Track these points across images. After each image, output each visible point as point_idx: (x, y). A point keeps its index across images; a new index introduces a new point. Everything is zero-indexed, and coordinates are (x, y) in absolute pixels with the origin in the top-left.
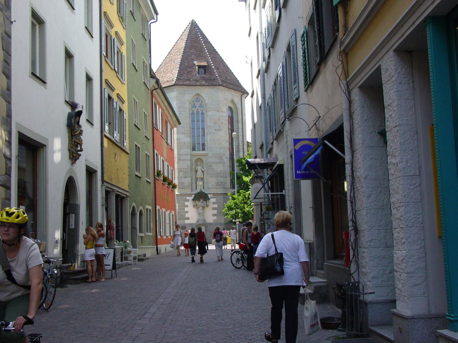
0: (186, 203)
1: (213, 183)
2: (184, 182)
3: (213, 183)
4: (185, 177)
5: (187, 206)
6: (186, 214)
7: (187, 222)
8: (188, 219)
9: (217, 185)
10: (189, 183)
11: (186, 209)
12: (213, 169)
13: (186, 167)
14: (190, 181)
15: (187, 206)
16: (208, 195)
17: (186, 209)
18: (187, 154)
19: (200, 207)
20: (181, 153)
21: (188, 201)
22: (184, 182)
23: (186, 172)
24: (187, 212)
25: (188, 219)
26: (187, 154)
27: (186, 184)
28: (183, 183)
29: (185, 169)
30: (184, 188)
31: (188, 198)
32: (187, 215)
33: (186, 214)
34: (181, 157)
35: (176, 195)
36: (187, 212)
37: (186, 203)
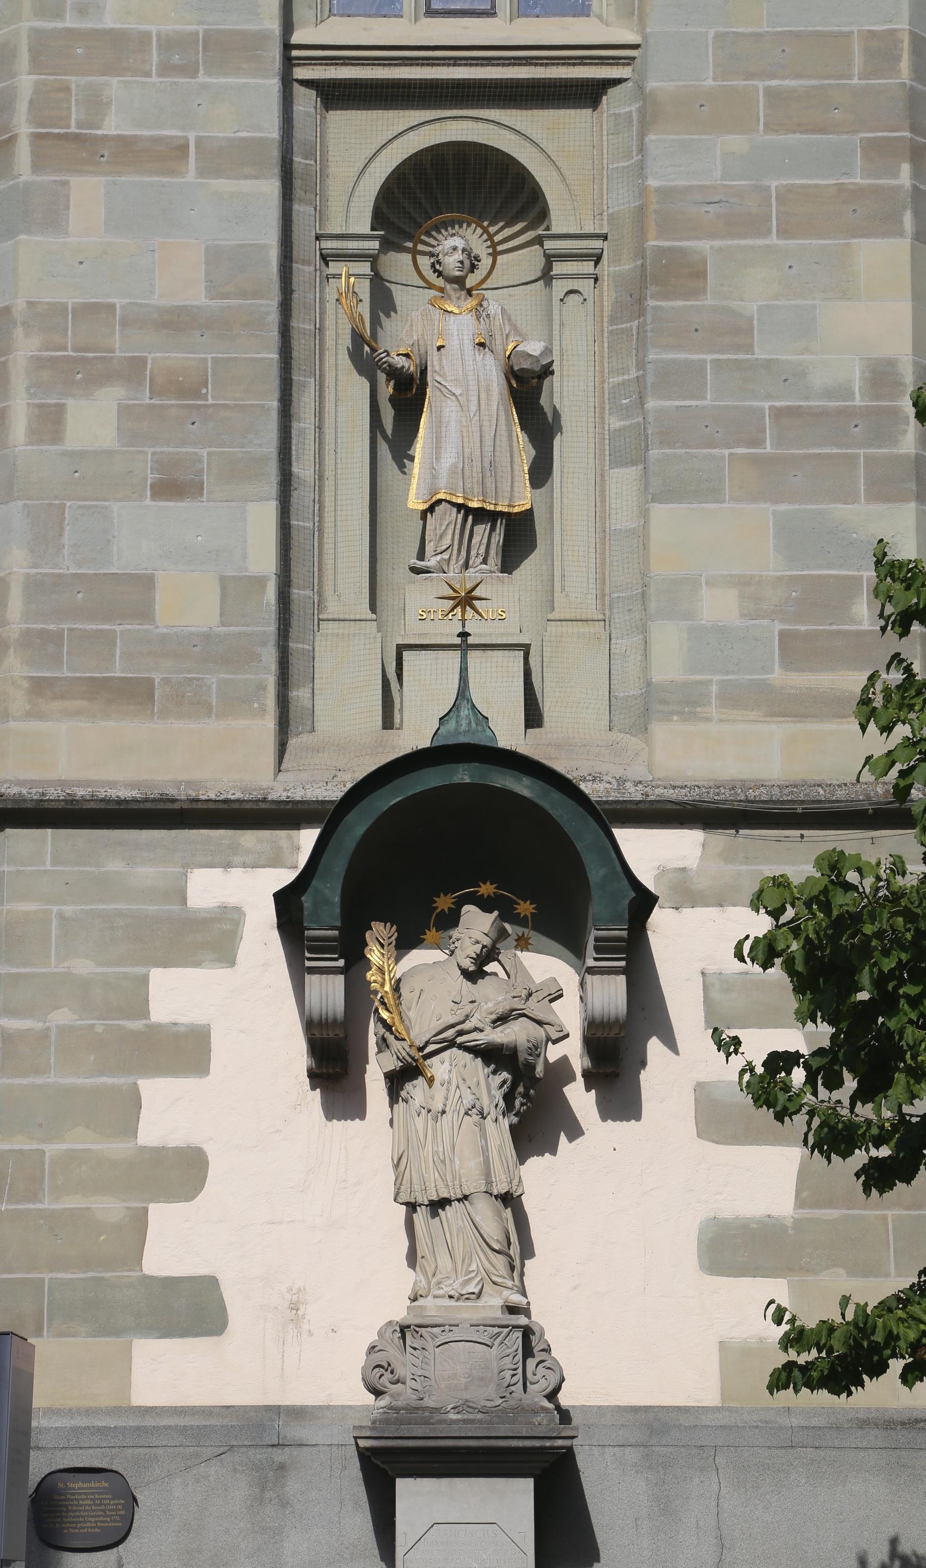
0: (175, 994)
1: (719, 607)
2: (145, 582)
3: (719, 607)
4: (174, 486)
5: (187, 1051)
6: (158, 1213)
7: (166, 1374)
8: (195, 1309)
9: (794, 649)
10: (234, 589)
11: (167, 1111)
12: (737, 331)
13: (197, 297)
14: (263, 559)
15: (187, 1051)
16: (626, 837)
17: (167, 1111)
18: (223, 49)
19: (440, 1067)
20: (109, 22)
21: (212, 939)
22: (146, 582)
23: (187, 388)
24: (185, 1172)
25: (195, 1309)
26: (223, 49)
27: (189, 604)
28: (134, 594)
29: (176, 322)
30: (134, 695)
31: (208, 888)
32: (174, 1243)
33: (158, 1213)
34: (96, 104)
35: (140, 970)
36: (185, 1172)
37: (175, 994)
